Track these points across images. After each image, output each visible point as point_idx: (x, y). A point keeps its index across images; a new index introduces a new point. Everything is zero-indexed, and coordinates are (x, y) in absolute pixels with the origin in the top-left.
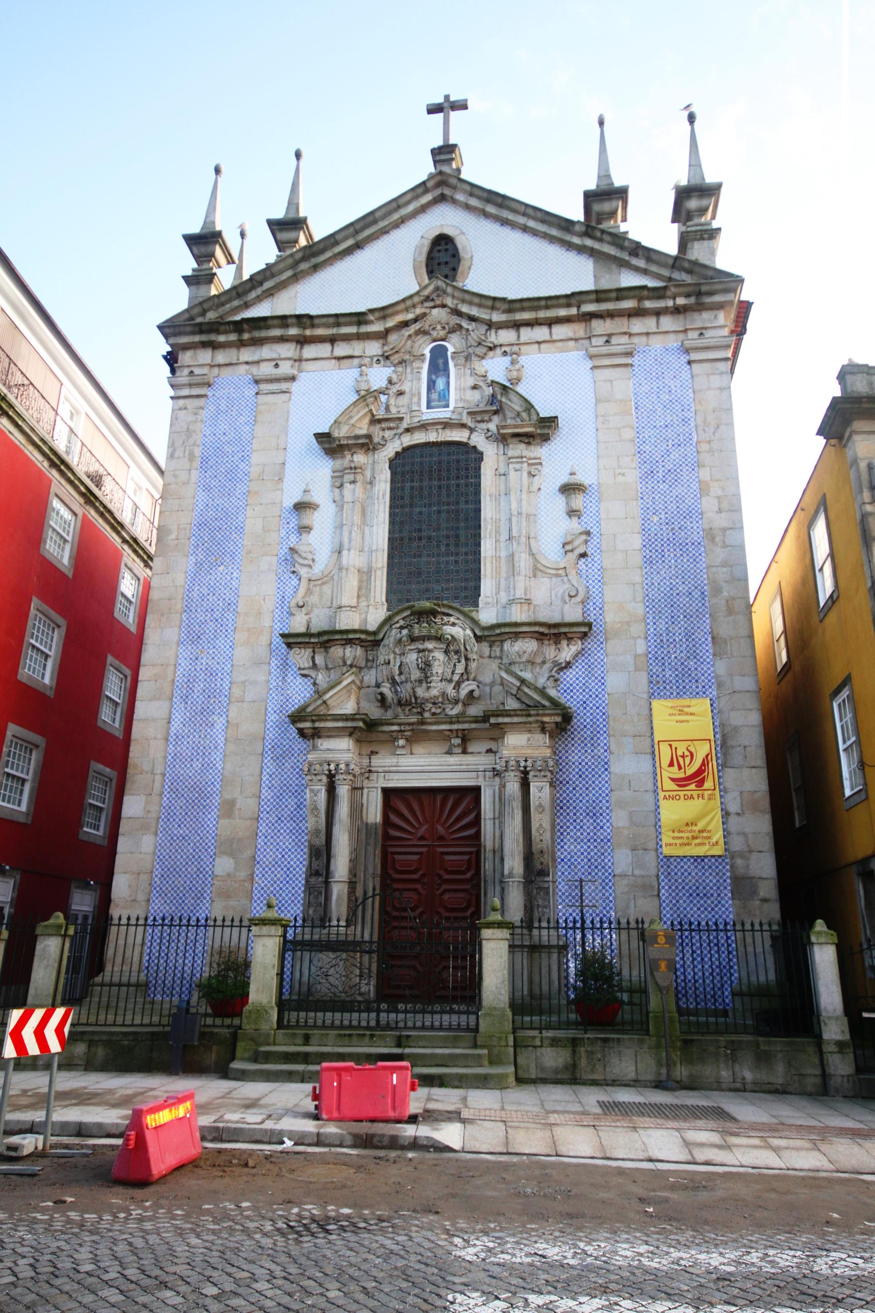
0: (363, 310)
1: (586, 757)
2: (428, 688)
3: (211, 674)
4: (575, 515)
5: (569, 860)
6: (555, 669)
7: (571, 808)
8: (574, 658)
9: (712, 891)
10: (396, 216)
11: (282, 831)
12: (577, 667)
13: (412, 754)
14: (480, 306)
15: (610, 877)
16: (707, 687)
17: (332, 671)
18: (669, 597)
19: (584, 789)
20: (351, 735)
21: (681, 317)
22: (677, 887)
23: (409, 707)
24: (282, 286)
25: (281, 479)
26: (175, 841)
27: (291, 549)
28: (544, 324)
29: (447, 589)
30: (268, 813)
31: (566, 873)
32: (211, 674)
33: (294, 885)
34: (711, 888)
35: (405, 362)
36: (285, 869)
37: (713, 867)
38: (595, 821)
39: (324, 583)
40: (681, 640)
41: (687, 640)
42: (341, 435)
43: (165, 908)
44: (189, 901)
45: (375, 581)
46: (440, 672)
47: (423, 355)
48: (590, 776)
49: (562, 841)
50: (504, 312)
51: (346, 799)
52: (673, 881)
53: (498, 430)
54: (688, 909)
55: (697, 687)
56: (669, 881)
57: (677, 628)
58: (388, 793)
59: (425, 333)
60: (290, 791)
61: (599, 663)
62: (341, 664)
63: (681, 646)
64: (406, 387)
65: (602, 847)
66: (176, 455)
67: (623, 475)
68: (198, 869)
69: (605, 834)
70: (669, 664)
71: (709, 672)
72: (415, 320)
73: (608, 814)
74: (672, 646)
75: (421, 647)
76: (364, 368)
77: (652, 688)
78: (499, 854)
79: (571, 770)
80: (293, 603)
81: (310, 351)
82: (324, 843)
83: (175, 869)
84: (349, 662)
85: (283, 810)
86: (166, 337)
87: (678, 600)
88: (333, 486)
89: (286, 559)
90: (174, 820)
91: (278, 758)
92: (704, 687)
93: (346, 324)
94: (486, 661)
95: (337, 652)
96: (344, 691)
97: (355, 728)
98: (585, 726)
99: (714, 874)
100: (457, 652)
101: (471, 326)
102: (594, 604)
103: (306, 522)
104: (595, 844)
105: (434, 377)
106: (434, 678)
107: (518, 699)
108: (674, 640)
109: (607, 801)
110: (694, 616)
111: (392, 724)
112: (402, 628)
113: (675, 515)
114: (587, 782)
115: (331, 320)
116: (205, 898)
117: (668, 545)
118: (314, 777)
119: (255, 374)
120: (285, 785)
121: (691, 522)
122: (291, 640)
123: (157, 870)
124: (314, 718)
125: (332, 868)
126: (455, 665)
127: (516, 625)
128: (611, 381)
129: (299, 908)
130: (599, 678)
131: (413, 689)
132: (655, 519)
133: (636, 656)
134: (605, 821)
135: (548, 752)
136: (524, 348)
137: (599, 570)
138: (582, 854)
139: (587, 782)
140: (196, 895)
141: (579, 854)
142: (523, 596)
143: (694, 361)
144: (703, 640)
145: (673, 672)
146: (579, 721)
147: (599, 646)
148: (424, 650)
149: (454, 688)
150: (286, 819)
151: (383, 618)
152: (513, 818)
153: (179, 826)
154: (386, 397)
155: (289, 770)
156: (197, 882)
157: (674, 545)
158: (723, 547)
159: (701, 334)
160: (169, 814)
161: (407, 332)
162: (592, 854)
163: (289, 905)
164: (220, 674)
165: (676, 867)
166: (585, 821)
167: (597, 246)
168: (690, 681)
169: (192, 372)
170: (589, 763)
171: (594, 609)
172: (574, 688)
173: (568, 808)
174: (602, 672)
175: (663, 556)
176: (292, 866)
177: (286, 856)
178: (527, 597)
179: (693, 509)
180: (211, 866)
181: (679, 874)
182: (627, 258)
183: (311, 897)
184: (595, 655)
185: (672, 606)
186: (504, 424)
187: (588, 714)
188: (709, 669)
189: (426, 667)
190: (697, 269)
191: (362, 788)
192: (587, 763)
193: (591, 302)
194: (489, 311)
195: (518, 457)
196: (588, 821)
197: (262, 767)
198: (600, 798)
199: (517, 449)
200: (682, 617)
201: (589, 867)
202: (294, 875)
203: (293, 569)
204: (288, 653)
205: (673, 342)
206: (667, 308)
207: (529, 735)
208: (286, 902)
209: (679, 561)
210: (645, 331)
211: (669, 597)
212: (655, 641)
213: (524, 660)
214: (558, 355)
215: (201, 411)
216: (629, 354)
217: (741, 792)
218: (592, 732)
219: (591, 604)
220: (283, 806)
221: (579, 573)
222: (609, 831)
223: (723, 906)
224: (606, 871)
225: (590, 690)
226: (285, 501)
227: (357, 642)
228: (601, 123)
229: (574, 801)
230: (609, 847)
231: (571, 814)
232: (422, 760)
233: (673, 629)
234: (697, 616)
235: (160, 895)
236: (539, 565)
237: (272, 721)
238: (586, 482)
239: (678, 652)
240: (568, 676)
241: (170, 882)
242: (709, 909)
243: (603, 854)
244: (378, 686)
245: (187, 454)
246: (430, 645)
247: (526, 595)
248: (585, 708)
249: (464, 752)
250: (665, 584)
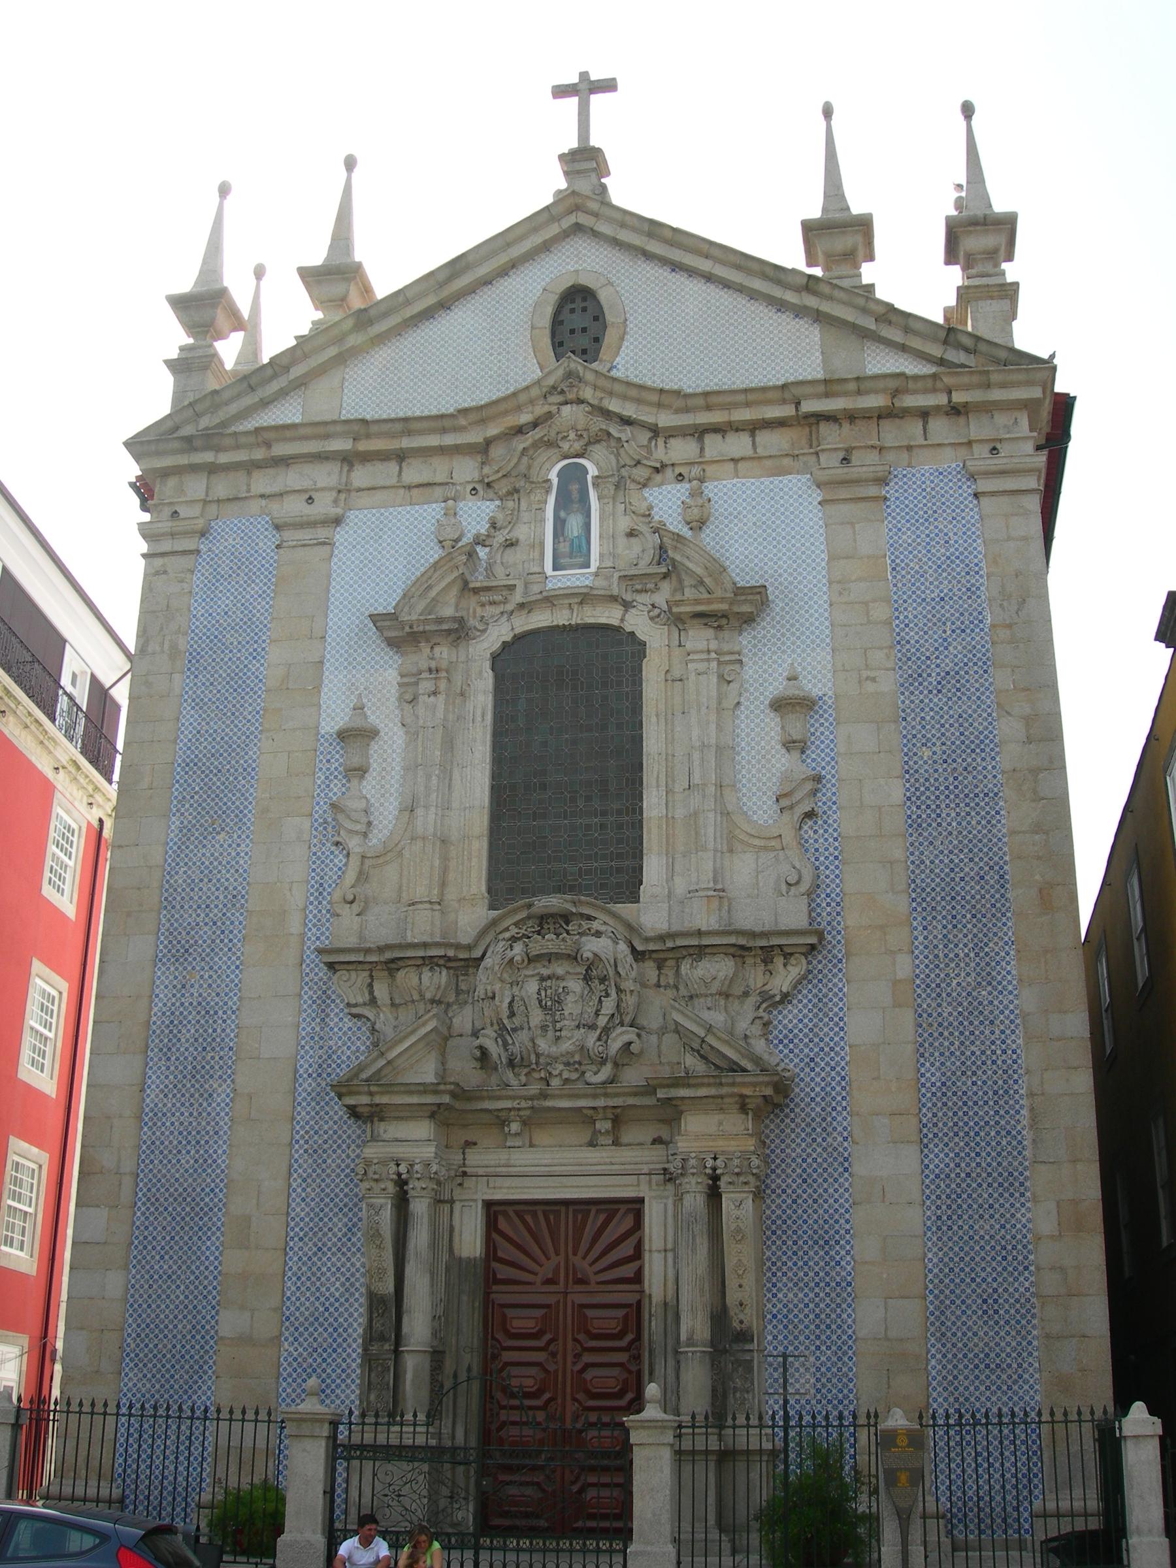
0: (451, 410)
1: (814, 1150)
2: (558, 1038)
3: (207, 1012)
4: (794, 748)
5: (786, 1316)
6: (764, 1005)
7: (790, 1232)
8: (795, 987)
9: (1009, 1361)
10: (503, 259)
11: (324, 1269)
12: (800, 1001)
13: (531, 1146)
14: (639, 401)
15: (850, 1343)
16: (1008, 1032)
17: (401, 1009)
18: (948, 884)
19: (810, 1201)
20: (432, 1116)
21: (962, 420)
22: (955, 1356)
23: (526, 1070)
24: (321, 371)
25: (318, 688)
26: (156, 1281)
27: (333, 806)
28: (743, 430)
29: (588, 872)
30: (301, 1239)
31: (780, 1337)
32: (207, 1012)
33: (344, 1355)
34: (1009, 1355)
35: (517, 491)
36: (331, 1330)
37: (1013, 1322)
38: (827, 1253)
39: (386, 863)
40: (967, 955)
41: (977, 955)
42: (414, 617)
43: (144, 1385)
44: (181, 1377)
45: (470, 860)
46: (577, 1012)
48: (820, 1180)
49: (774, 1285)
50: (678, 411)
51: (426, 1220)
52: (949, 1345)
53: (670, 608)
54: (972, 1388)
55: (993, 1033)
56: (944, 1345)
57: (960, 936)
58: (493, 1210)
59: (551, 444)
60: (336, 1205)
61: (836, 995)
62: (416, 997)
63: (967, 965)
64: (522, 532)
65: (838, 1295)
66: (150, 649)
67: (874, 680)
68: (194, 1327)
69: (844, 1274)
70: (949, 995)
71: (1011, 1007)
72: (535, 424)
73: (848, 1242)
74: (953, 965)
75: (545, 972)
76: (451, 502)
77: (920, 1035)
78: (672, 1311)
79: (789, 1171)
80: (337, 895)
81: (361, 476)
82: (391, 1288)
83: (157, 1326)
84: (428, 996)
85: (325, 1235)
86: (138, 458)
87: (963, 888)
88: (400, 699)
89: (325, 822)
90: (154, 1248)
91: (315, 1151)
92: (1003, 1032)
93: (421, 432)
94: (650, 992)
95: (407, 978)
96: (421, 1045)
97: (439, 1105)
98: (813, 1099)
99: (1013, 1333)
100: (603, 980)
101: (626, 433)
102: (828, 895)
103: (356, 761)
104: (828, 1290)
105: (562, 514)
106: (566, 1022)
107: (702, 1057)
108: (957, 955)
109: (847, 1221)
110: (989, 915)
111: (499, 1098)
112: (514, 939)
113: (958, 747)
114: (815, 1191)
115: (399, 427)
116: (205, 1372)
117: (947, 797)
118: (373, 1184)
119: (275, 514)
120: (328, 1195)
121: (983, 759)
122: (332, 958)
123: (130, 1326)
124: (373, 1089)
125: (405, 1329)
126: (600, 1001)
127: (699, 933)
128: (852, 524)
129: (353, 1392)
130: (837, 1019)
131: (532, 1040)
132: (927, 753)
133: (896, 983)
134: (843, 1253)
135: (750, 1144)
136: (710, 470)
137: (836, 839)
138: (807, 1305)
139: (815, 1191)
140: (191, 1367)
141: (801, 1306)
142: (711, 885)
143: (983, 493)
144: (1003, 954)
145: (955, 1009)
146: (802, 1090)
147: (835, 966)
148: (549, 977)
149: (599, 1039)
150: (329, 1249)
151: (484, 922)
152: (694, 1250)
153: (162, 1257)
154: (487, 550)
155: (333, 1171)
156: (193, 1347)
157: (957, 796)
158: (1034, 801)
159: (994, 449)
160: (145, 1238)
161: (520, 443)
162: (822, 1305)
163: (338, 1386)
164: (220, 1013)
165: (954, 1323)
166: (811, 1253)
167: (826, 307)
168: (981, 1023)
169: (176, 512)
170: (819, 1160)
171: (828, 904)
172: (796, 1036)
173: (785, 1232)
174: (841, 1009)
175: (939, 816)
176: (341, 1325)
177: (332, 1310)
178: (719, 886)
179: (986, 737)
180: (213, 1322)
181: (959, 1334)
182: (873, 327)
183: (373, 1375)
184: (830, 981)
185: (953, 898)
186: (678, 597)
187: (818, 1080)
188: (1011, 1002)
189: (552, 1005)
190: (982, 347)
191: (452, 1202)
192: (815, 1160)
193: (819, 396)
194: (655, 410)
195: (702, 652)
196: (816, 1253)
197: (291, 1166)
198: (837, 1217)
199: (699, 638)
200: (969, 916)
201: (818, 1326)
202: (345, 1340)
203: (336, 839)
204: (330, 979)
205: (949, 461)
206: (938, 406)
207: (722, 1117)
208: (334, 1381)
209: (964, 823)
210: (905, 443)
211: (948, 884)
212: (926, 957)
213: (713, 990)
214: (767, 481)
215: (189, 576)
216: (883, 481)
217: (1058, 1203)
218: (823, 1109)
219: (823, 896)
220: (326, 1230)
221: (802, 844)
222: (849, 1268)
223: (1026, 1382)
224: (845, 1332)
225: (821, 1040)
226: (323, 724)
227: (441, 962)
229: (795, 1222)
230: (849, 1295)
231: (790, 1243)
232: (547, 1156)
233: (955, 936)
234: (994, 915)
235: (136, 1365)
236: (737, 832)
237: (305, 1090)
238: (816, 692)
239: (963, 974)
240: (785, 1017)
241: (151, 1346)
242: (1005, 1388)
243: (839, 1305)
244: (475, 1034)
245: (166, 646)
246: (559, 969)
247: (715, 881)
248: (813, 1070)
249: (616, 1143)
250: (941, 861)
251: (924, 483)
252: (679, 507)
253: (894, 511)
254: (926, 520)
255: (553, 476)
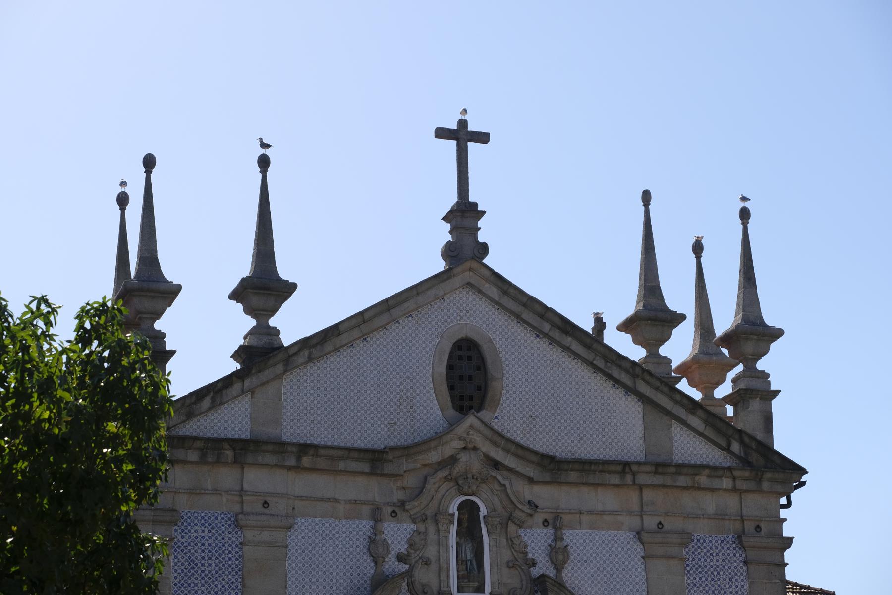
47: (453, 515)
64: (431, 552)
251: (711, 548)
252: (546, 548)
253: (691, 569)
254: (713, 579)
255: (453, 508)
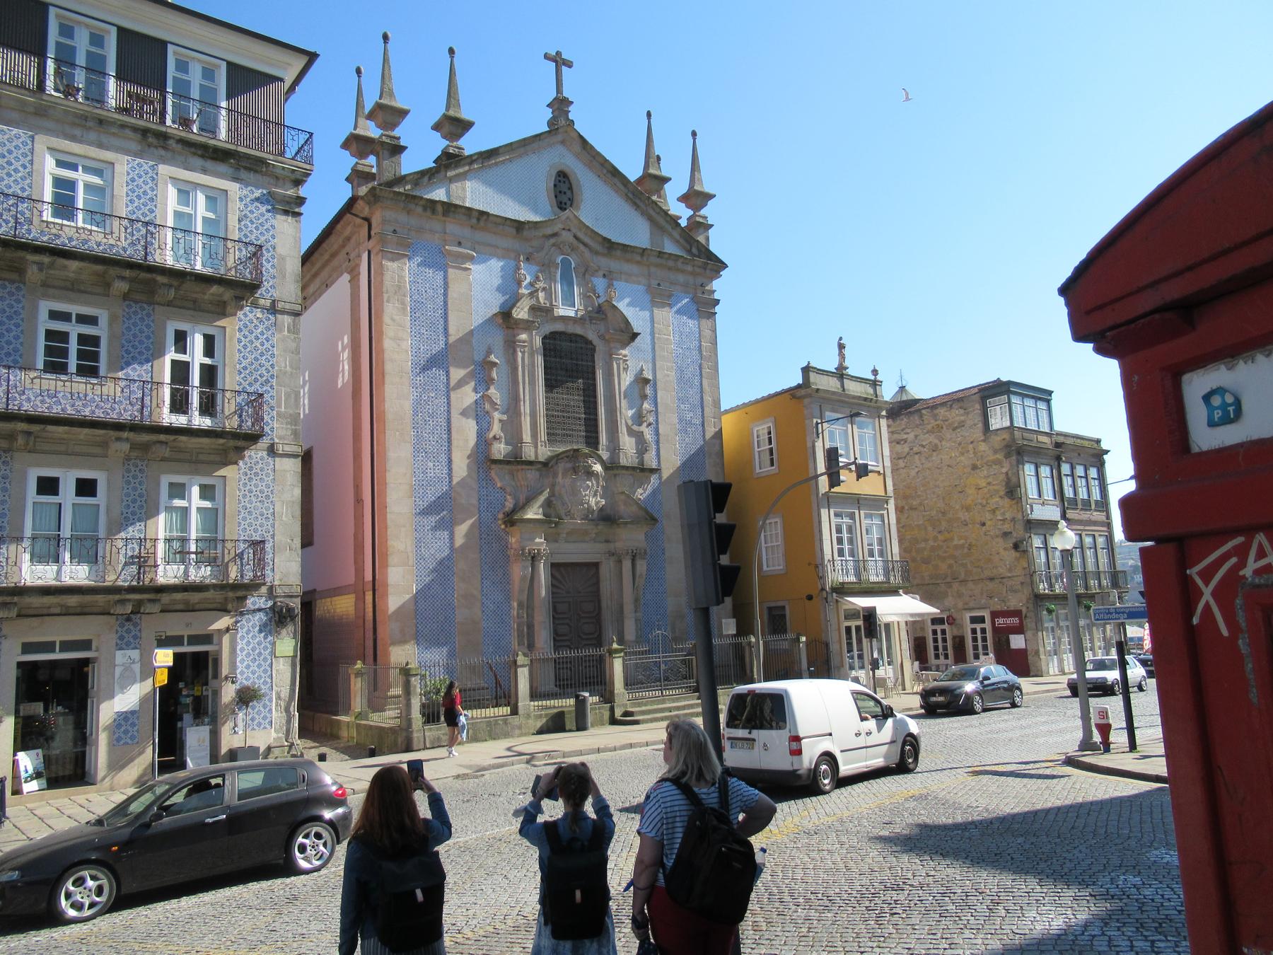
101: (586, 251)
228: (649, 115)
